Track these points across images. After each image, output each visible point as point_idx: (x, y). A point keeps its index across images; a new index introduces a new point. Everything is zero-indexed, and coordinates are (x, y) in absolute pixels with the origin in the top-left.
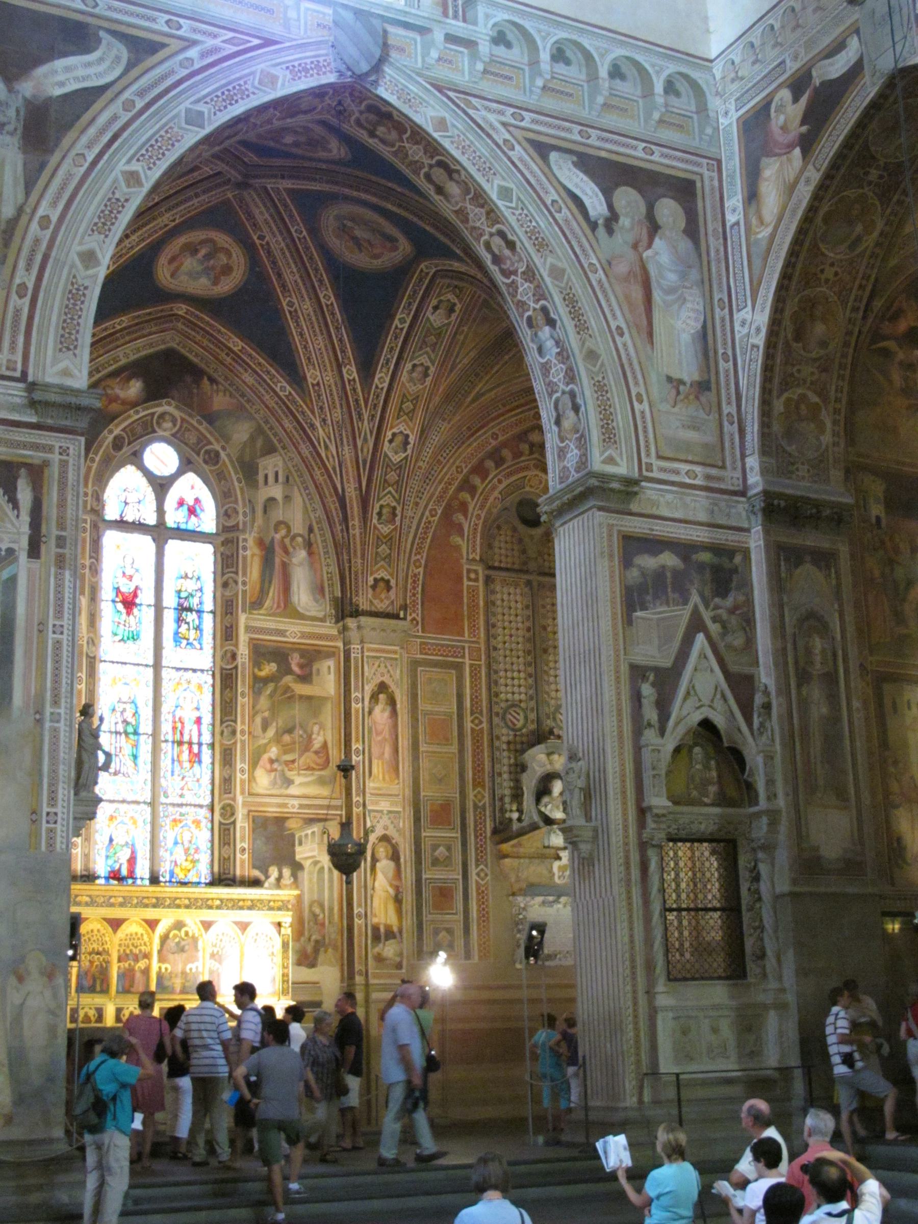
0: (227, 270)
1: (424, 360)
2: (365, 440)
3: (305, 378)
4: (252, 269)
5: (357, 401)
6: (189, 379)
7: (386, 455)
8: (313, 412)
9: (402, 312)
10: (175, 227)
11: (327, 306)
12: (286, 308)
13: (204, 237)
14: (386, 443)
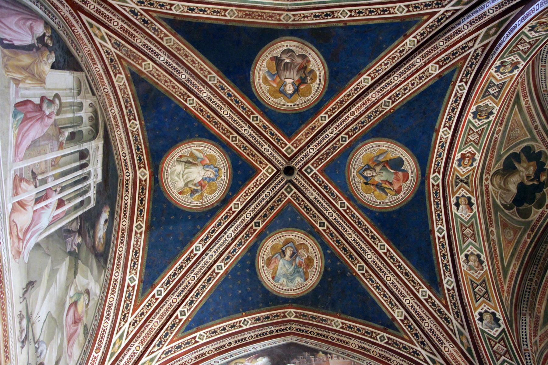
0: (310, 261)
1: (470, 249)
2: (461, 334)
3: (394, 319)
4: (325, 254)
5: (439, 311)
6: (307, 354)
7: (483, 332)
8: (411, 342)
9: (437, 225)
10: (261, 231)
11: (385, 253)
12: (359, 272)
13: (285, 238)
14: (478, 322)
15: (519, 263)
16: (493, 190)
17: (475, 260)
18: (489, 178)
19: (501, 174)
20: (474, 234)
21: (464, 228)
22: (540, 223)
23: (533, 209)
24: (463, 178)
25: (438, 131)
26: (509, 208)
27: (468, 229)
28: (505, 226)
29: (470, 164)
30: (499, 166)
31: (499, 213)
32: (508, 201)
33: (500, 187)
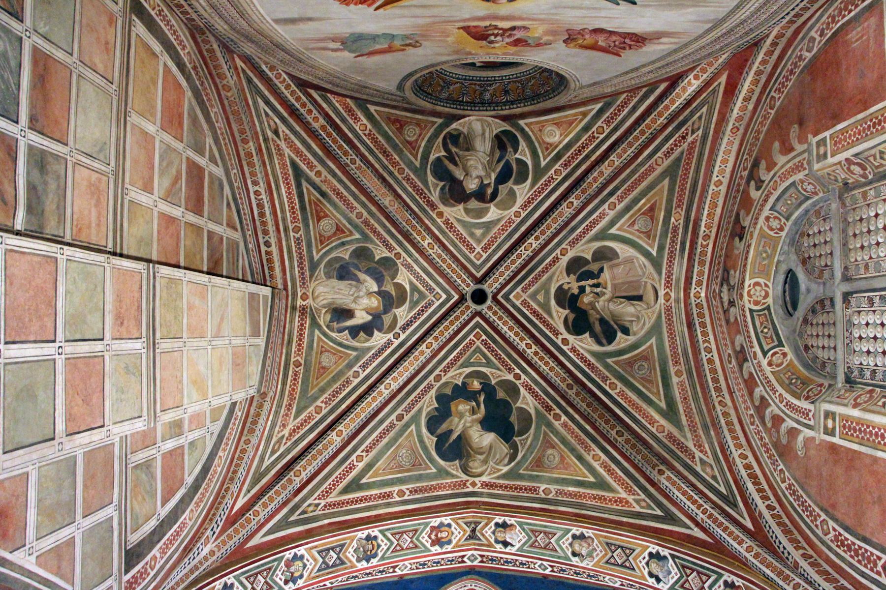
15: (593, 446)
16: (489, 474)
17: (580, 545)
18: (471, 479)
19: (467, 460)
20: (545, 533)
21: (537, 544)
22: (540, 393)
23: (518, 404)
24: (468, 530)
25: (401, 576)
26: (515, 448)
27: (538, 539)
28: (539, 464)
29: (447, 529)
30: (453, 467)
31: (521, 471)
32: (506, 451)
33: (485, 462)
